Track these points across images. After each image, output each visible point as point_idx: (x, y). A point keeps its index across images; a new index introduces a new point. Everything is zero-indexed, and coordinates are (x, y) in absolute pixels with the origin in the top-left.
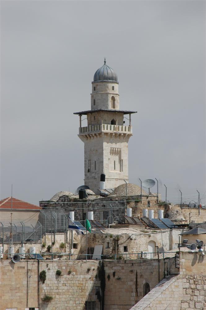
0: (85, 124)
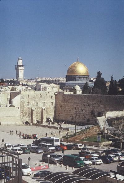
0: (16, 67)
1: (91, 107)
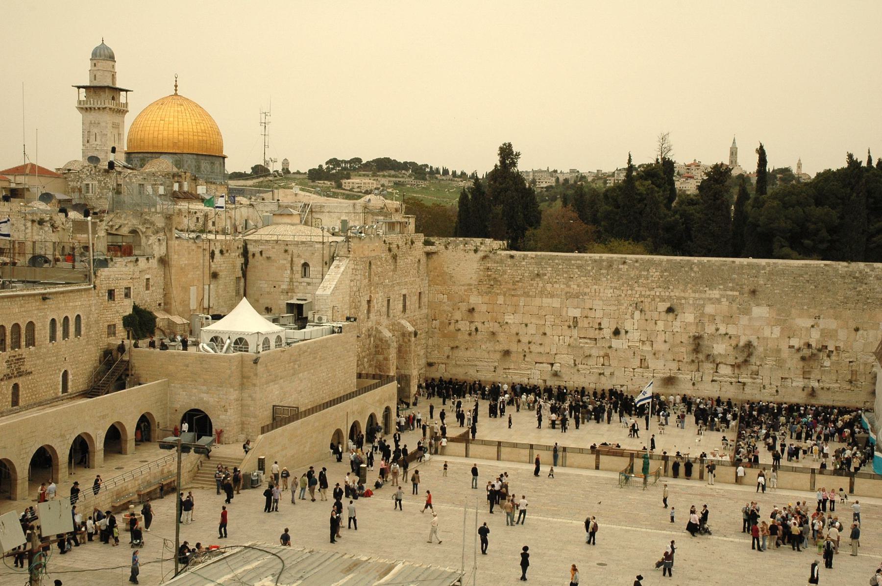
0: (83, 97)
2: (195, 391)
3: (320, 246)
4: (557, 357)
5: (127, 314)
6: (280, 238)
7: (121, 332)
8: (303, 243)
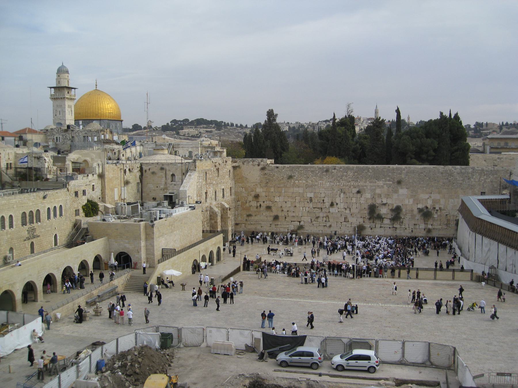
0: (53, 93)
1: (368, 196)
2: (122, 242)
3: (180, 165)
4: (302, 218)
5: (84, 204)
6: (159, 161)
7: (82, 213)
8: (171, 164)
